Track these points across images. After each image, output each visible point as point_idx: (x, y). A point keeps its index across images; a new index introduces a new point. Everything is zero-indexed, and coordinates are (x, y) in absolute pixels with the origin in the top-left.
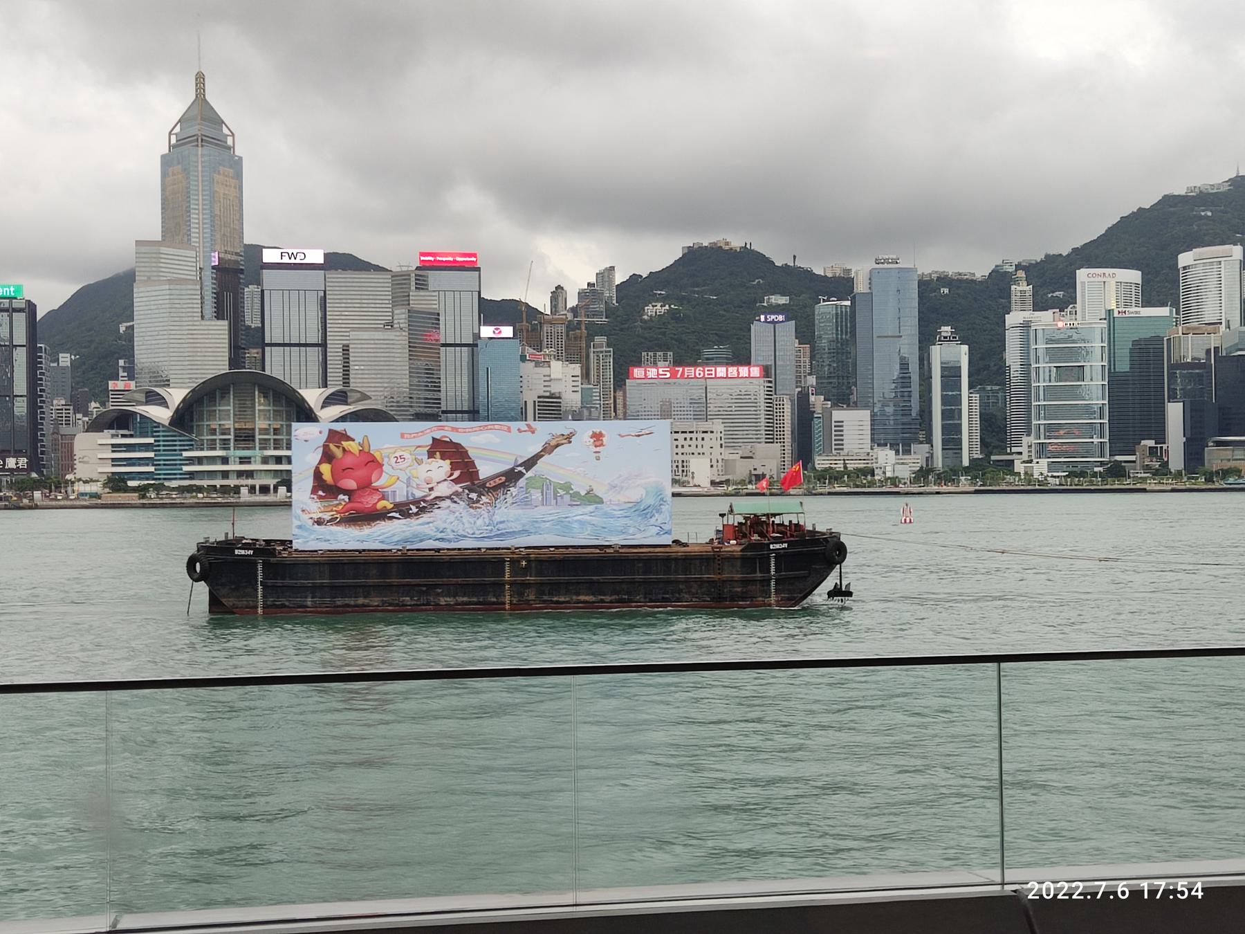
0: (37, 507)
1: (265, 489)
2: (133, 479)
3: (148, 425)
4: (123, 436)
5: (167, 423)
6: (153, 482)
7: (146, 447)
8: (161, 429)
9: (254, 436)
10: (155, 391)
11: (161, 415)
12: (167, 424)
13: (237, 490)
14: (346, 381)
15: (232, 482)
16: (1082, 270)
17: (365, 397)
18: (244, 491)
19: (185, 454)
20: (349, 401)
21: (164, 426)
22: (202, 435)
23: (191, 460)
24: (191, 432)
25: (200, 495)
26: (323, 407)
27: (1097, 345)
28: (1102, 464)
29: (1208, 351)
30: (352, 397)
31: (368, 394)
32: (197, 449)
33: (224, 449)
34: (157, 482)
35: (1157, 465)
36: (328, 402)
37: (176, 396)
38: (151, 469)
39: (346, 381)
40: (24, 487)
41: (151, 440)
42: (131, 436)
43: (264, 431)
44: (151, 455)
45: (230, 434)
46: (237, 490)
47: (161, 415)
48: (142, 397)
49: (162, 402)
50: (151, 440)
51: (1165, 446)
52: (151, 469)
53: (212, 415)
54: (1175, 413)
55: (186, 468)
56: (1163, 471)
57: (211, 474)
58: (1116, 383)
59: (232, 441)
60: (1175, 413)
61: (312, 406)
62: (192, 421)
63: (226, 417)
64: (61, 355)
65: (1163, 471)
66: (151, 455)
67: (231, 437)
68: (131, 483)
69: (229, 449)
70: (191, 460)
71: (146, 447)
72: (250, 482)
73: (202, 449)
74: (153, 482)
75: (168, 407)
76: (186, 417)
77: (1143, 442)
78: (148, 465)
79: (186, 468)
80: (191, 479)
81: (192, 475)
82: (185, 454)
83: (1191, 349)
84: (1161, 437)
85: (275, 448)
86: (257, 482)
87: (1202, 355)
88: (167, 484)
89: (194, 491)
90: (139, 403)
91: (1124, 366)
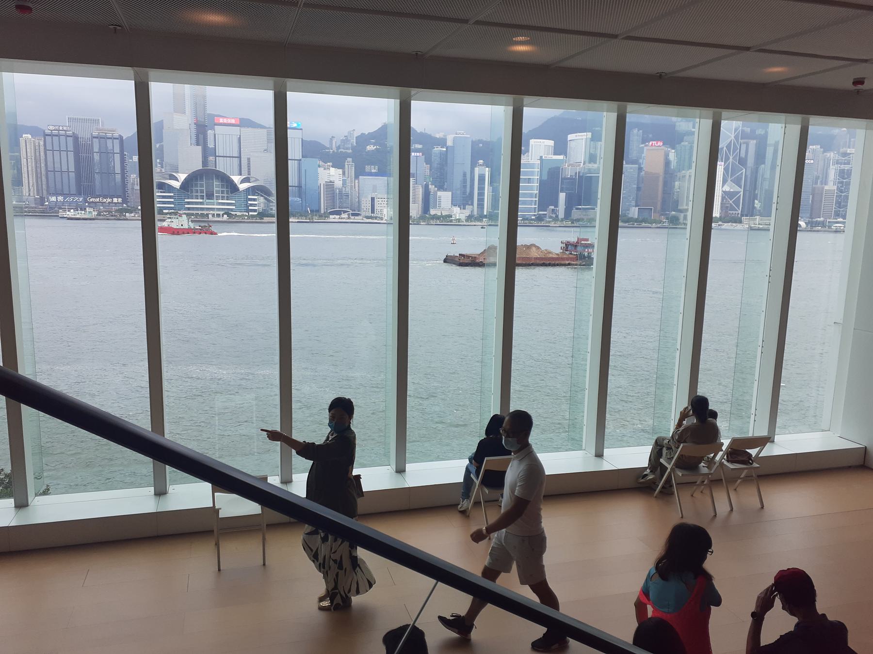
0: (127, 220)
1: (218, 215)
2: (165, 209)
3: (170, 188)
4: (161, 192)
5: (178, 188)
6: (173, 211)
7: (170, 197)
8: (176, 190)
9: (213, 194)
10: (173, 175)
11: (176, 184)
12: (178, 188)
13: (207, 215)
14: (249, 174)
15: (205, 212)
16: (532, 140)
17: (257, 180)
18: (210, 216)
19: (186, 200)
20: (251, 181)
21: (177, 189)
22: (193, 193)
23: (189, 203)
24: (188, 192)
25: (193, 217)
26: (240, 183)
27: (537, 170)
28: (535, 215)
29: (576, 173)
30: (252, 180)
31: (258, 178)
32: (191, 199)
33: (202, 199)
34: (175, 211)
35: (554, 216)
36: (243, 181)
37: (182, 177)
38: (173, 206)
39: (249, 174)
40: (122, 211)
41: (172, 194)
42: (164, 192)
43: (217, 192)
44: (172, 200)
45: (203, 193)
46: (207, 215)
47: (176, 184)
48: (167, 176)
49: (176, 179)
50: (172, 194)
51: (557, 209)
52: (173, 206)
53: (196, 185)
54: (562, 196)
55: (186, 206)
56: (556, 219)
57: (197, 209)
58: (542, 183)
59: (205, 196)
60: (562, 196)
61: (236, 183)
62: (188, 187)
63: (202, 186)
64: (133, 157)
65: (556, 219)
66: (172, 200)
67: (205, 194)
68: (164, 211)
69: (203, 199)
70: (189, 203)
71: (170, 197)
72: (211, 212)
73: (193, 199)
74: (173, 211)
75: (178, 181)
76: (187, 185)
77: (550, 207)
78: (171, 204)
79: (186, 206)
80: (189, 210)
81: (189, 209)
82: (186, 200)
83: (569, 172)
84: (556, 206)
85: (222, 199)
86: (216, 213)
87: (574, 174)
88: (179, 212)
89: (190, 215)
90: (167, 179)
91: (545, 177)
